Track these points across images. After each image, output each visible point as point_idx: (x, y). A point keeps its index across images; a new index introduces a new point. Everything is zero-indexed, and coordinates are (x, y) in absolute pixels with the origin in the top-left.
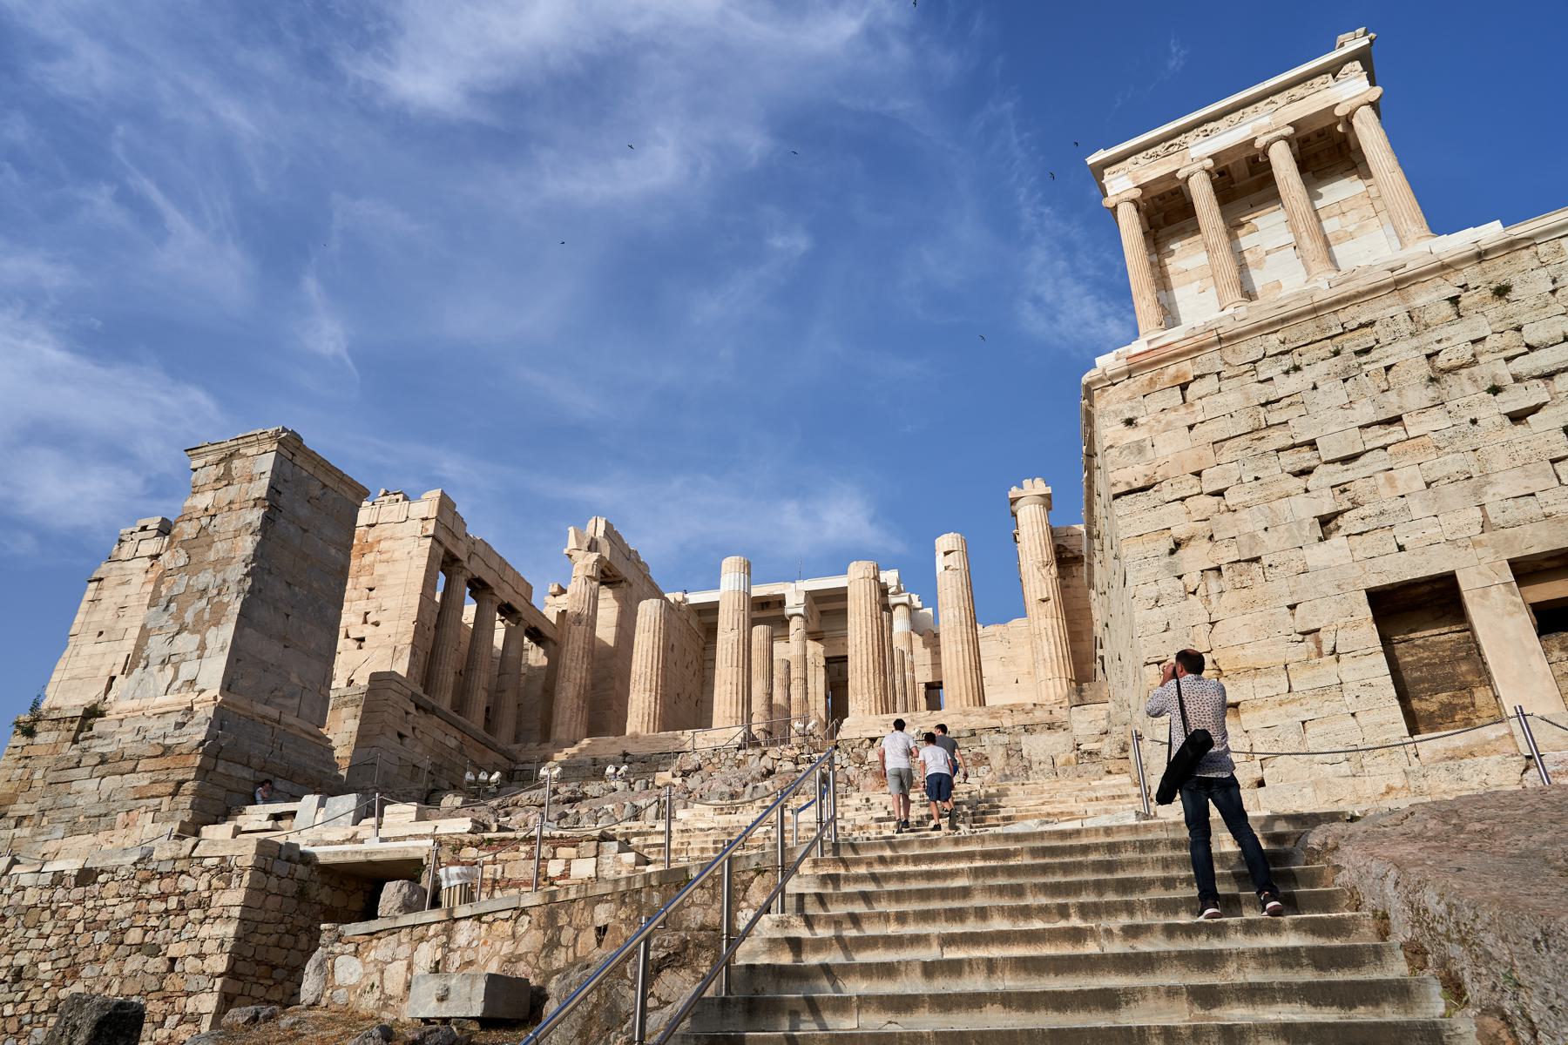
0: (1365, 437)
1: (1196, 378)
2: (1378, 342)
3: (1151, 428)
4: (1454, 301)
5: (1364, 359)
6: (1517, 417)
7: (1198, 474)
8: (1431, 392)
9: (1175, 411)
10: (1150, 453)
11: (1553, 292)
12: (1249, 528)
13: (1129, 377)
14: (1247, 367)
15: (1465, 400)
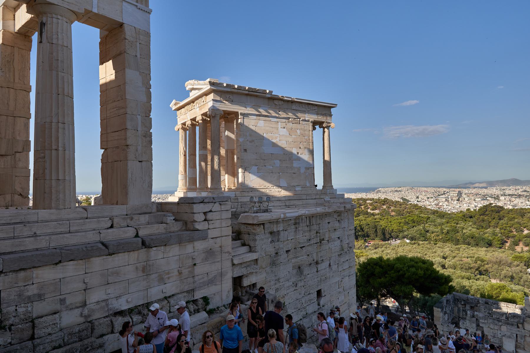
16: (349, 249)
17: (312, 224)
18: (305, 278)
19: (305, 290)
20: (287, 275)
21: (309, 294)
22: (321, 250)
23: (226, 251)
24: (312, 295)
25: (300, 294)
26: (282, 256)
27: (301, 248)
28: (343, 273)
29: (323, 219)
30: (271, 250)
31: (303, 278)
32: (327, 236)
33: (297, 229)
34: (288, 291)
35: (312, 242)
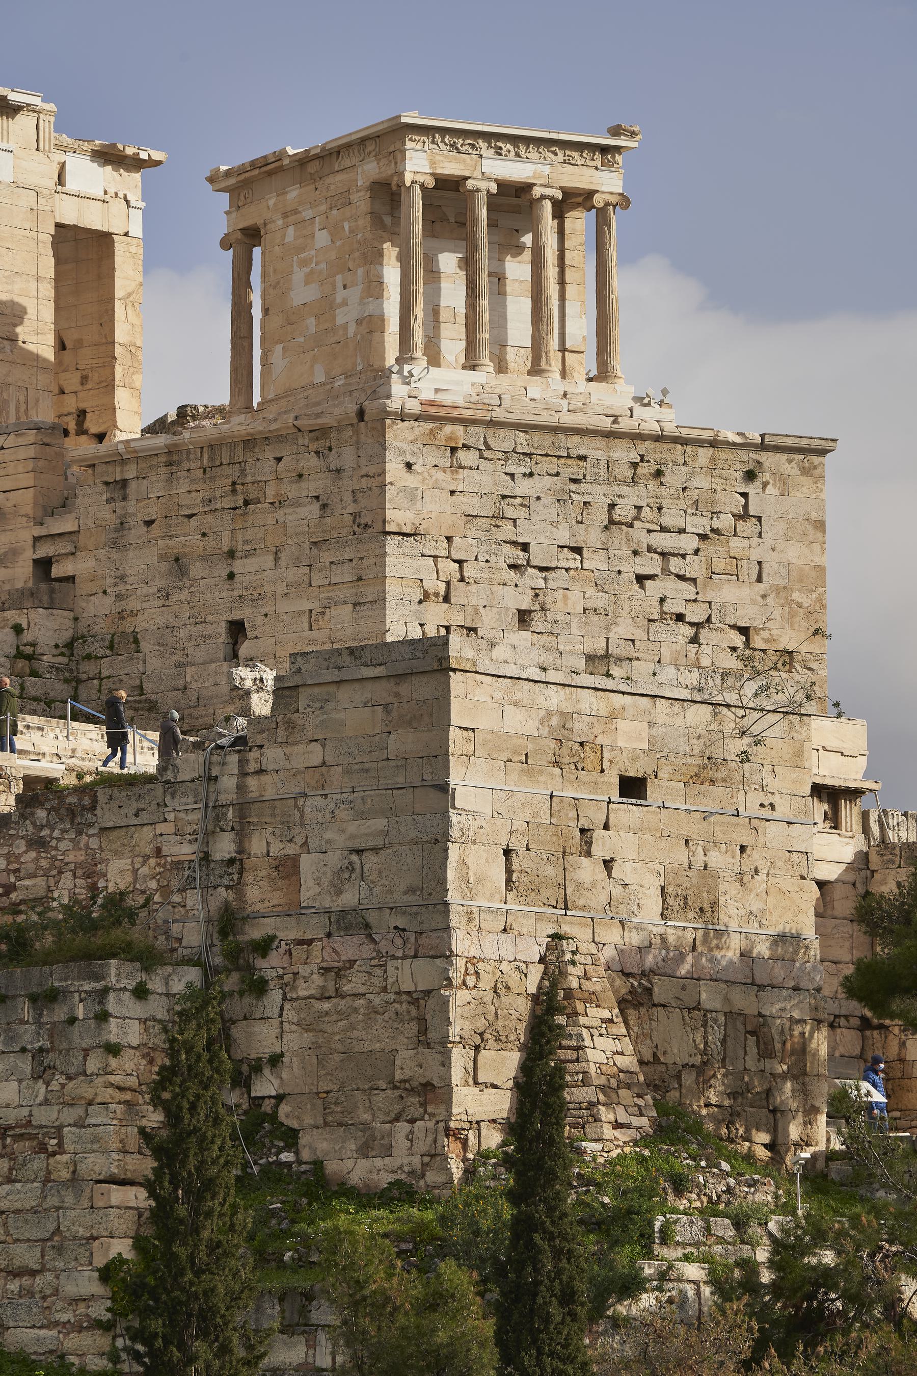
0: (561, 556)
1: (464, 446)
2: (585, 476)
3: (424, 479)
4: (635, 465)
5: (573, 487)
6: (641, 579)
7: (449, 539)
8: (603, 536)
9: (445, 472)
10: (419, 504)
11: (684, 489)
12: (474, 601)
13: (416, 420)
14: (500, 455)
15: (620, 553)
16: (356, 529)
17: (218, 463)
18: (192, 586)
19: (192, 611)
20: (146, 571)
21: (201, 622)
22: (249, 524)
23: (23, 513)
24: (208, 626)
25: (176, 617)
26: (133, 531)
27: (190, 516)
28: (328, 591)
29: (256, 450)
30: (106, 515)
31: (188, 583)
32: (271, 491)
33: (174, 476)
34: (145, 605)
35: (219, 506)
